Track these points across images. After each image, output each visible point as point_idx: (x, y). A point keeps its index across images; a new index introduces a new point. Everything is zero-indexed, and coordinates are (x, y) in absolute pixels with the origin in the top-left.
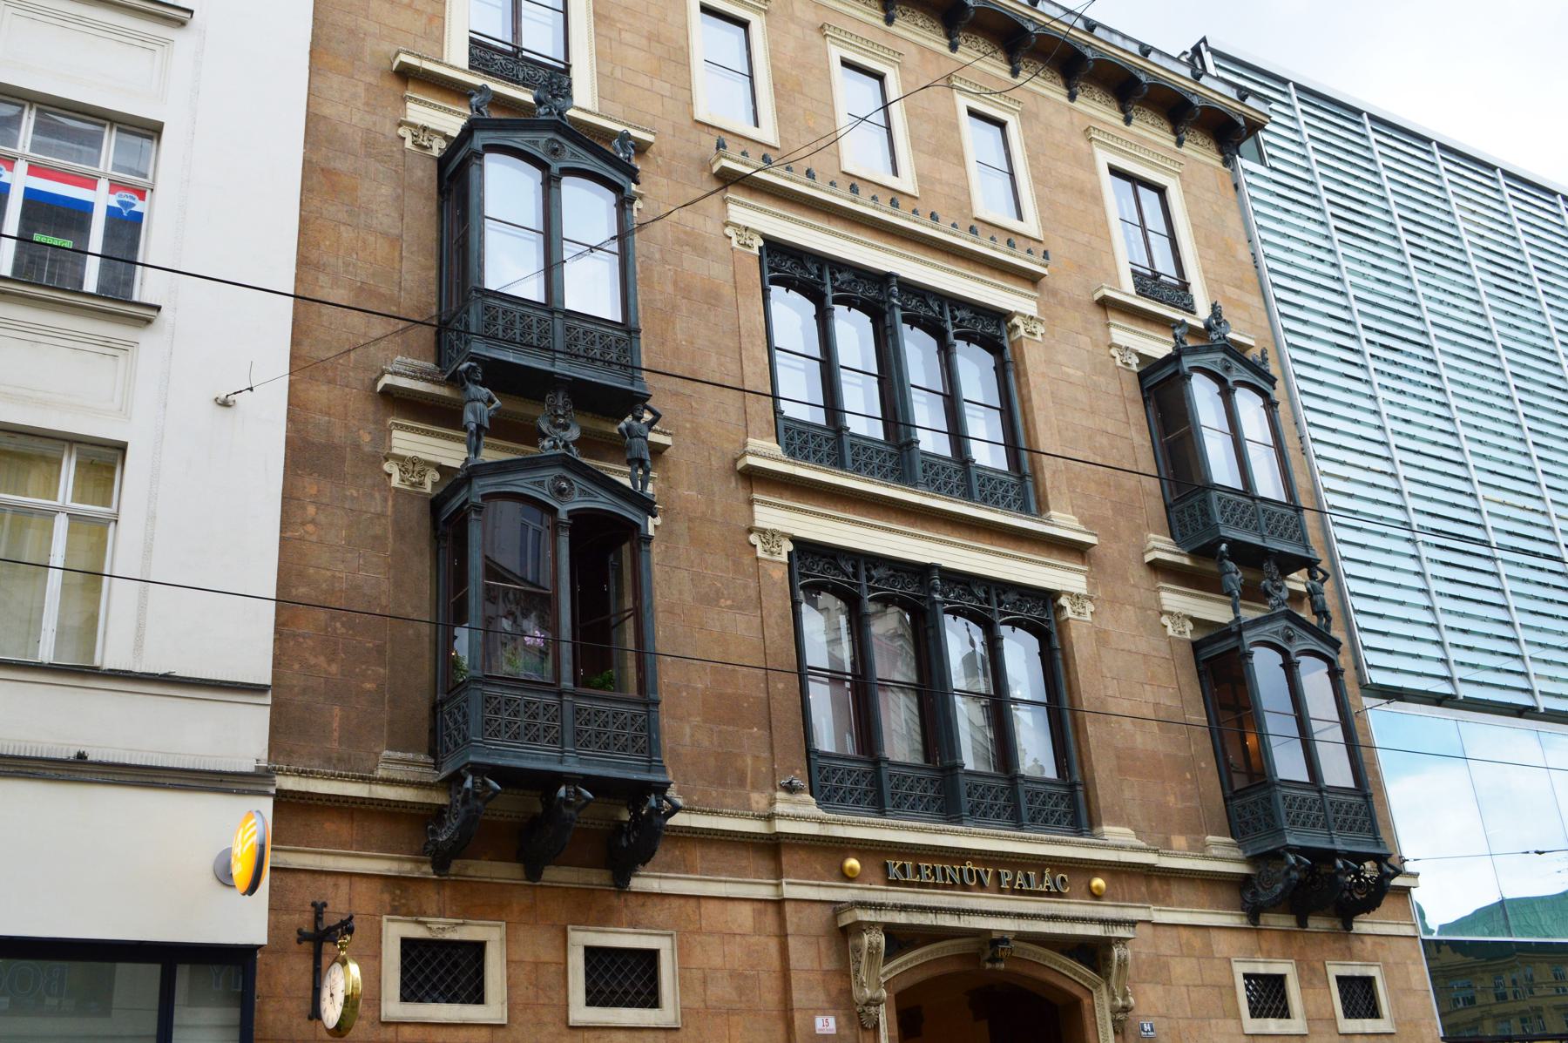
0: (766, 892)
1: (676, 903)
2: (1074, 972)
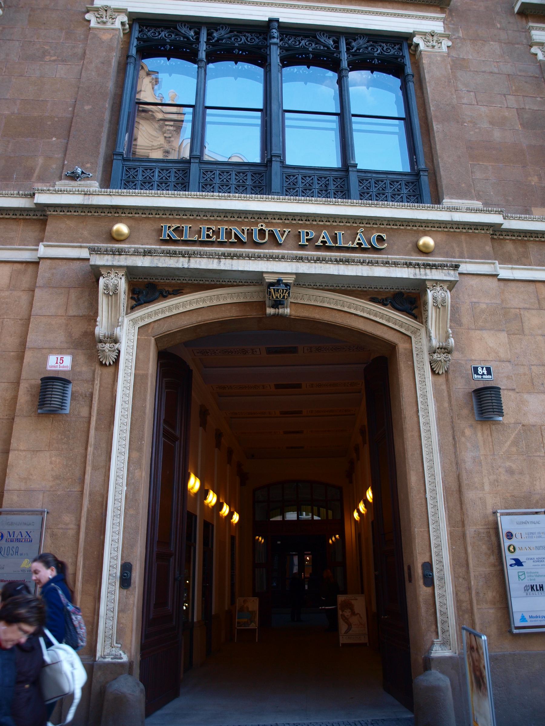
0: (26, 256)
2: (385, 320)
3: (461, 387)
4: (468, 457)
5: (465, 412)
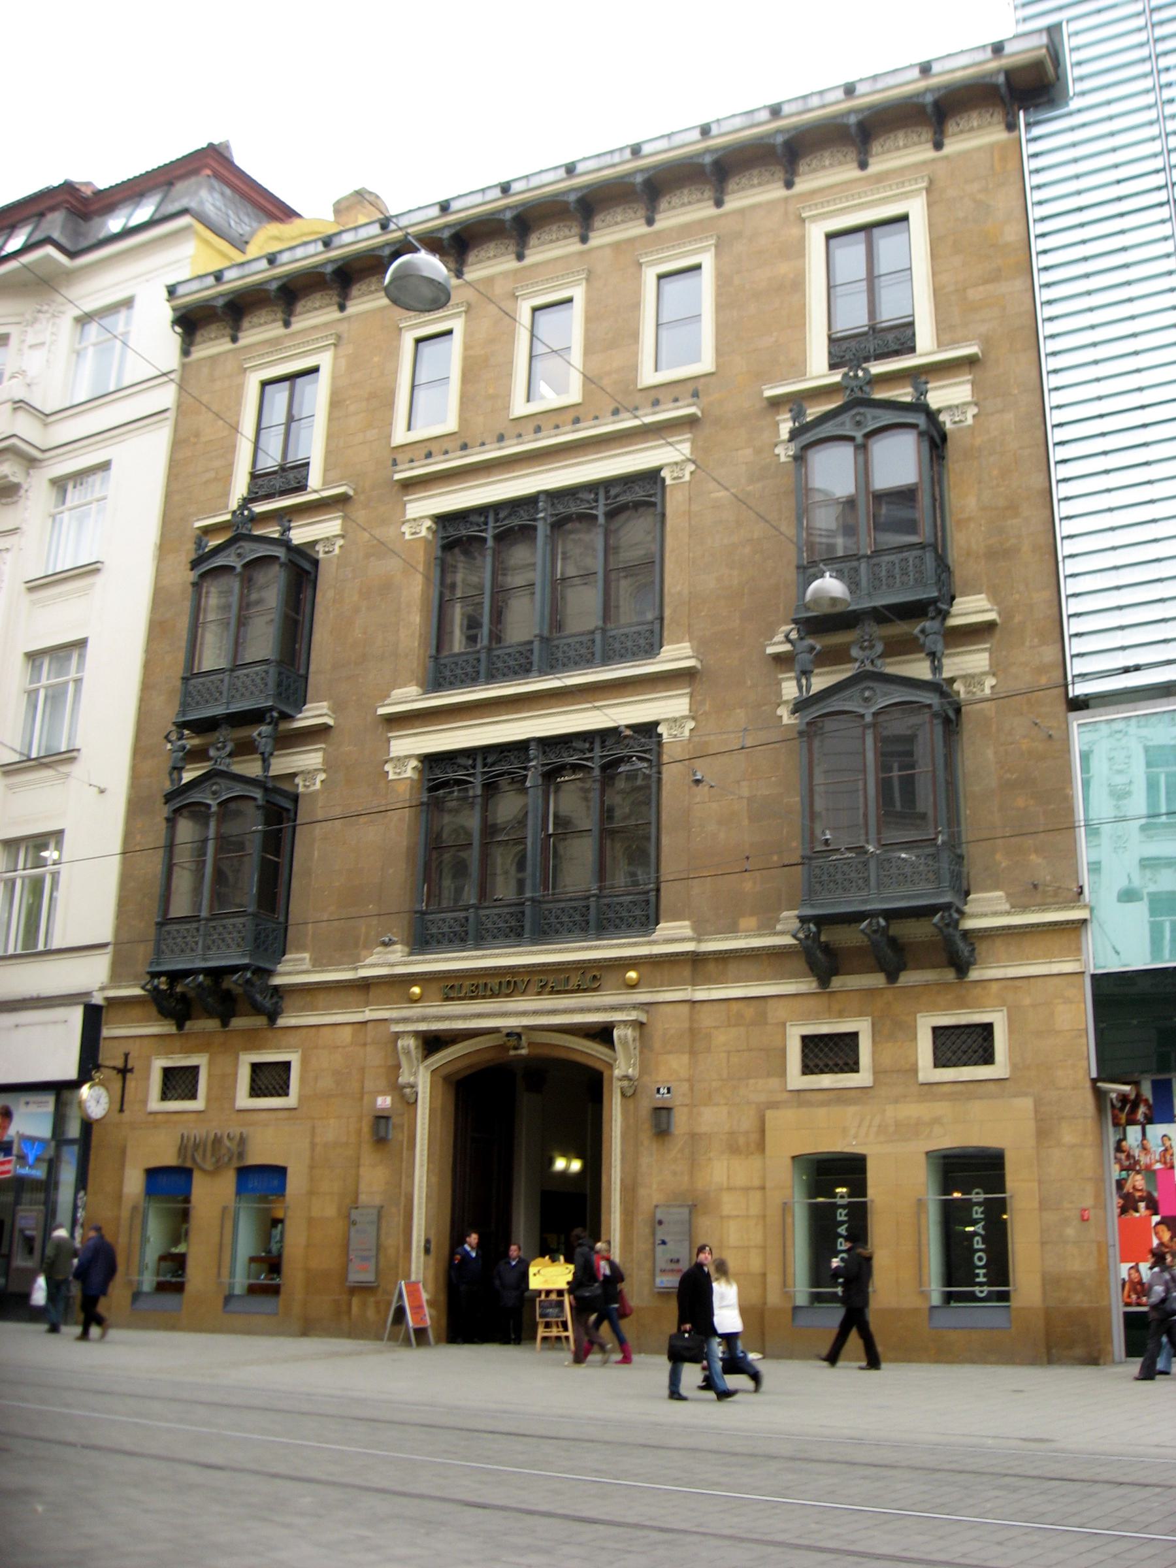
1: (305, 1031)
3: (645, 1105)
4: (645, 1160)
5: (646, 1126)
